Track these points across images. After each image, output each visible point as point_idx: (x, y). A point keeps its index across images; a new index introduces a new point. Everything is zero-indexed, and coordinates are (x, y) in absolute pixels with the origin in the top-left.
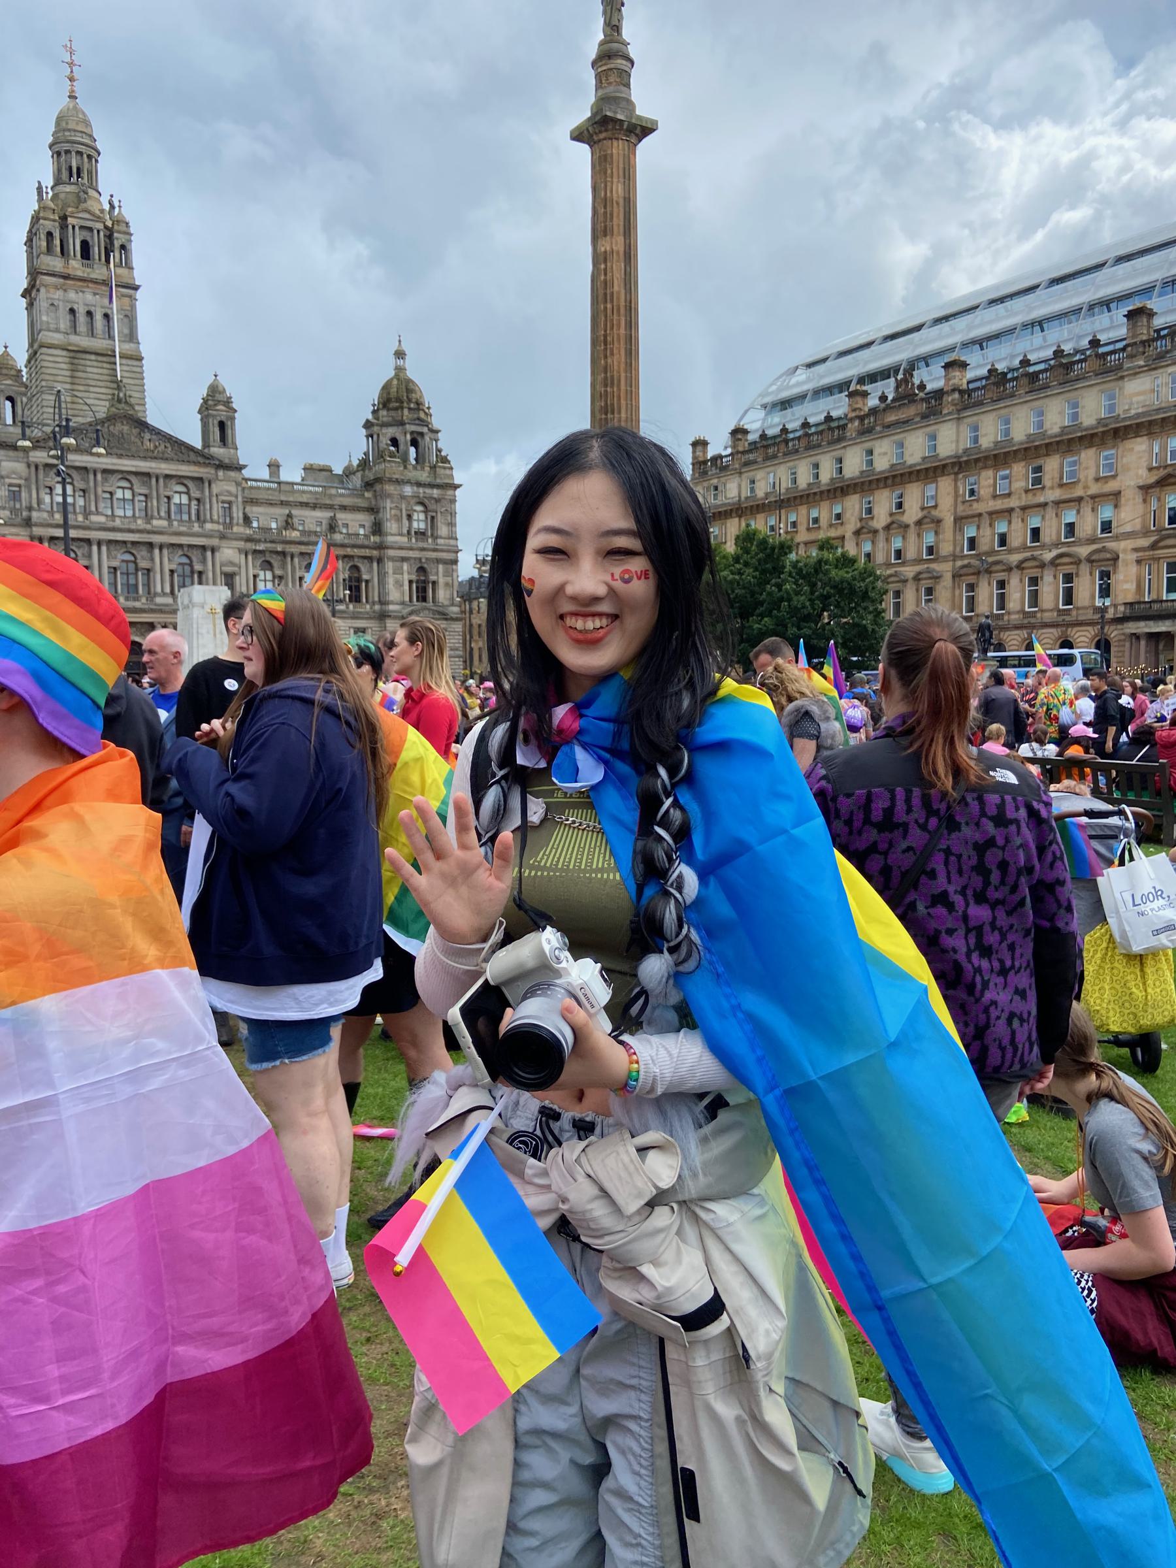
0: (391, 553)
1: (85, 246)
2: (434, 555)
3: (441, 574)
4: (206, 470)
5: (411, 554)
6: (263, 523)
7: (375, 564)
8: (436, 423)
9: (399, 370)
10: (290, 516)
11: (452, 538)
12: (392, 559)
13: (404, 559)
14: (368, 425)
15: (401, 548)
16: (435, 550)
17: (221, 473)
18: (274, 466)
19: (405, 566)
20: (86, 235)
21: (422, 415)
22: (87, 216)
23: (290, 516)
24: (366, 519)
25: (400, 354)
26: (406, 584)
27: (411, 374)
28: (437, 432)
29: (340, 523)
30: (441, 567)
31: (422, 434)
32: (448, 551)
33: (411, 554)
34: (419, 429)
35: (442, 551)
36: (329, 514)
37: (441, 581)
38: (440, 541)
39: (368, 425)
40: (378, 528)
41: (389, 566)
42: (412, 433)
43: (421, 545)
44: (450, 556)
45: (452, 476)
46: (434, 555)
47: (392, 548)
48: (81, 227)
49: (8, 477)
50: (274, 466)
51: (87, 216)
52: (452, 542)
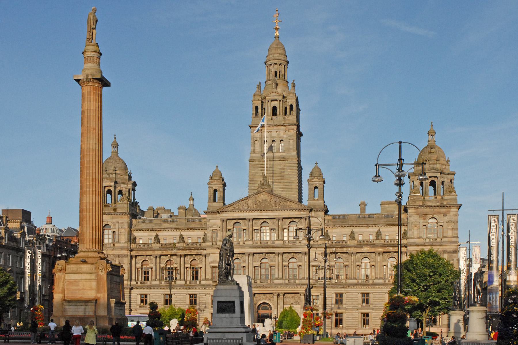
1: (274, 109)
4: (305, 213)
6: (340, 239)
10: (353, 233)
11: (454, 237)
17: (313, 214)
18: (363, 205)
20: (274, 103)
22: (275, 94)
23: (353, 233)
29: (382, 233)
36: (376, 229)
45: (456, 200)
48: (272, 101)
49: (212, 227)
50: (363, 205)
51: (275, 94)
52: (454, 240)
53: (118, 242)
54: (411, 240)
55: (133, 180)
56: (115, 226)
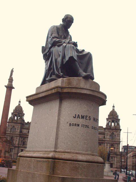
0: (106, 142)
2: (115, 142)
3: (116, 146)
5: (110, 142)
7: (103, 144)
8: (119, 118)
9: (113, 109)
12: (106, 143)
13: (109, 143)
14: (107, 119)
15: (108, 141)
16: (115, 141)
19: (109, 144)
21: (115, 117)
24: (103, 136)
25: (114, 107)
26: (109, 147)
27: (115, 110)
28: (119, 120)
30: (116, 145)
31: (114, 120)
32: (118, 142)
33: (110, 142)
34: (114, 119)
35: (116, 142)
37: (116, 147)
38: (116, 140)
39: (107, 119)
40: (104, 137)
41: (105, 144)
42: (112, 120)
43: (112, 140)
44: (119, 143)
46: (115, 142)
47: (106, 141)
52: (119, 140)
53: (16, 132)
54: (106, 139)
55: (24, 113)
56: (16, 126)
